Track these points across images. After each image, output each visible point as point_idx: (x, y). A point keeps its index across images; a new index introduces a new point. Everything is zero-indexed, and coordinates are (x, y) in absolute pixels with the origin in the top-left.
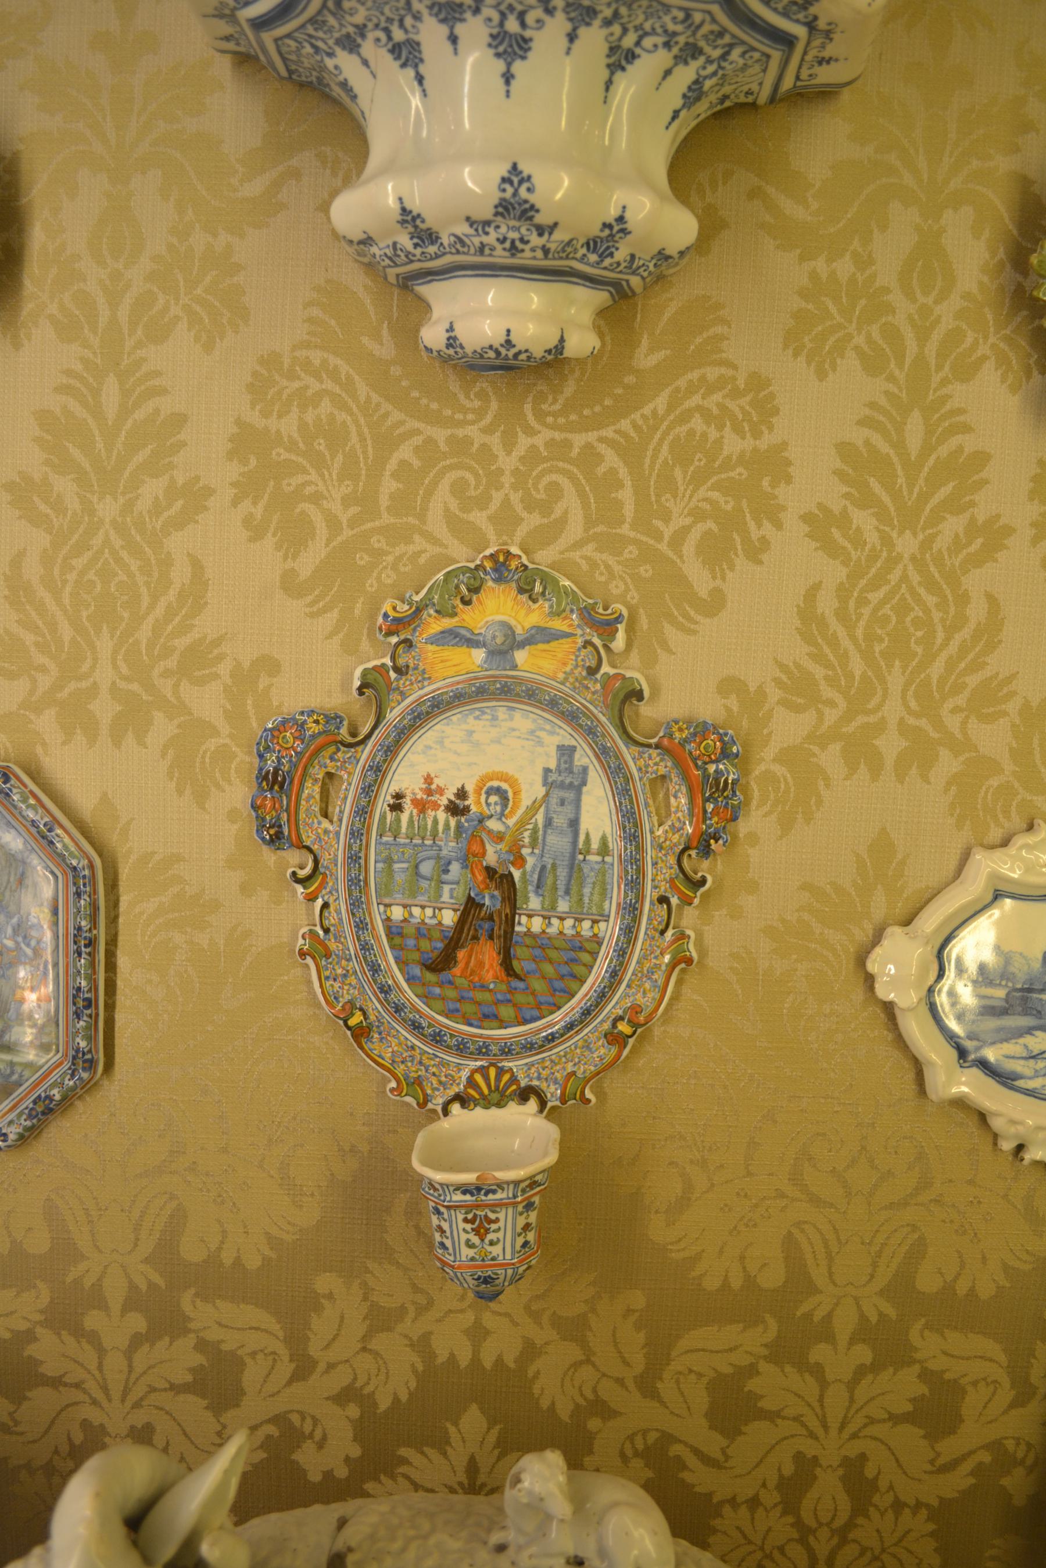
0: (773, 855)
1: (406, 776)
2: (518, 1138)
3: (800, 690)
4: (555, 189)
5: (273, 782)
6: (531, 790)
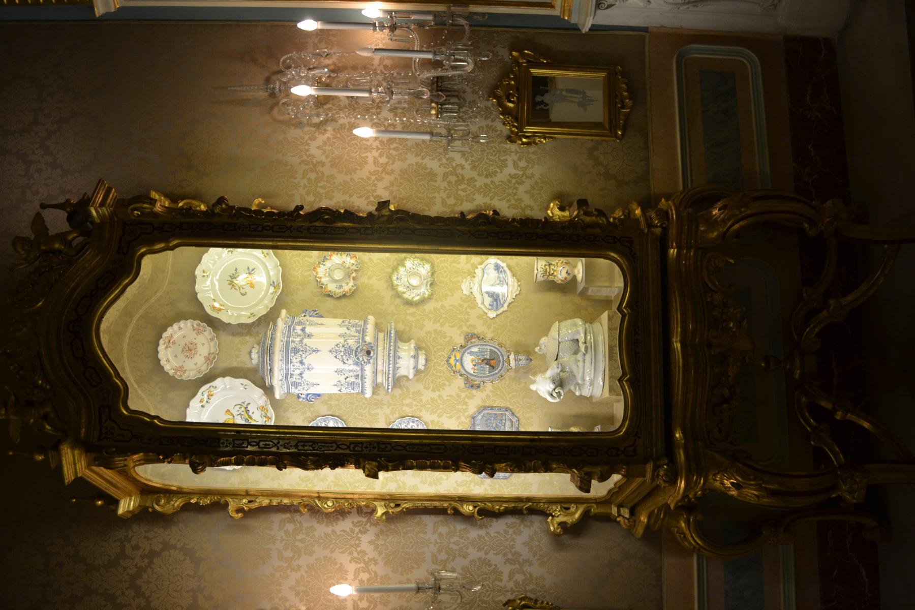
0: (480, 329)
1: (471, 371)
2: (512, 357)
3: (460, 327)
4: (412, 353)
5: (472, 386)
6: (472, 357)
